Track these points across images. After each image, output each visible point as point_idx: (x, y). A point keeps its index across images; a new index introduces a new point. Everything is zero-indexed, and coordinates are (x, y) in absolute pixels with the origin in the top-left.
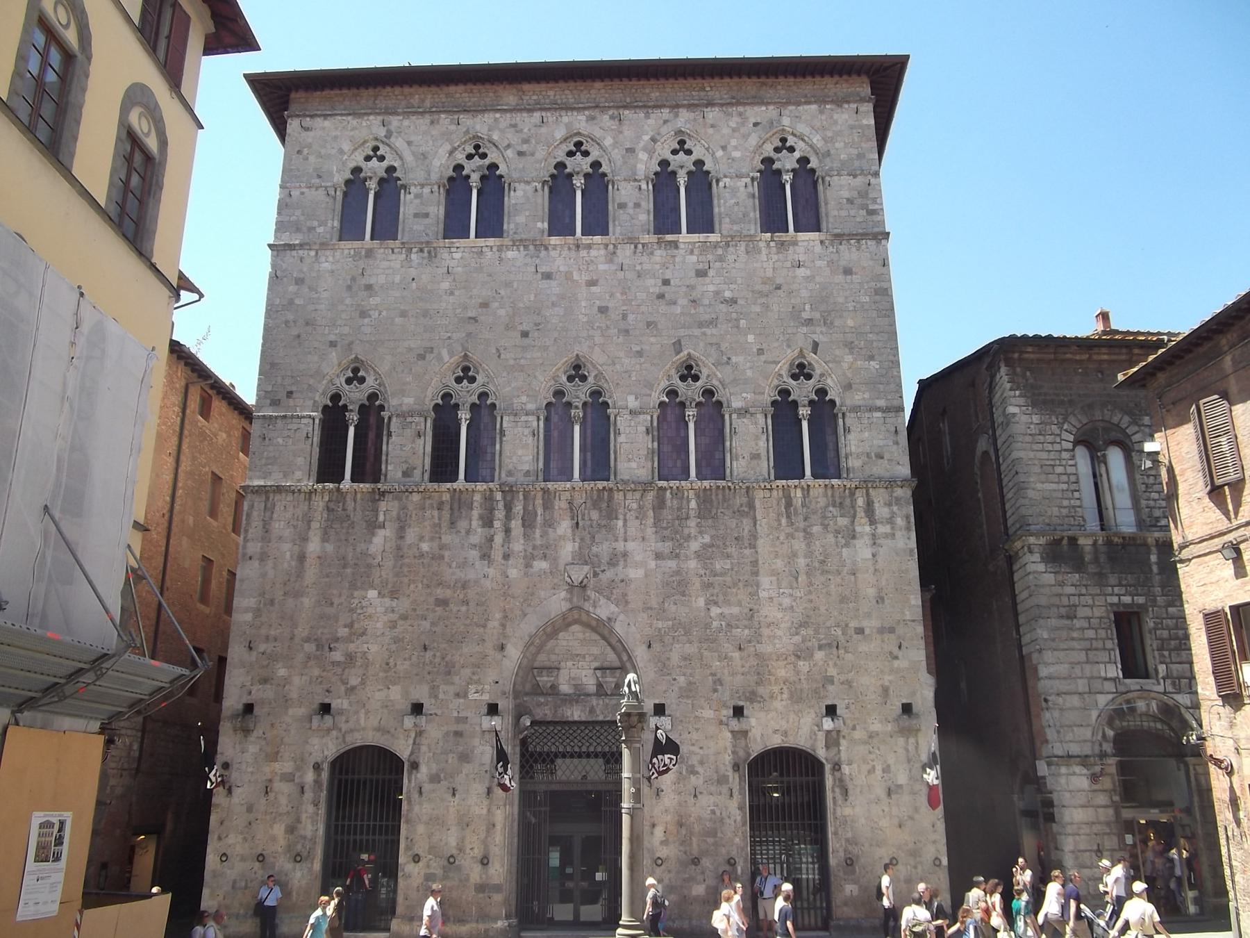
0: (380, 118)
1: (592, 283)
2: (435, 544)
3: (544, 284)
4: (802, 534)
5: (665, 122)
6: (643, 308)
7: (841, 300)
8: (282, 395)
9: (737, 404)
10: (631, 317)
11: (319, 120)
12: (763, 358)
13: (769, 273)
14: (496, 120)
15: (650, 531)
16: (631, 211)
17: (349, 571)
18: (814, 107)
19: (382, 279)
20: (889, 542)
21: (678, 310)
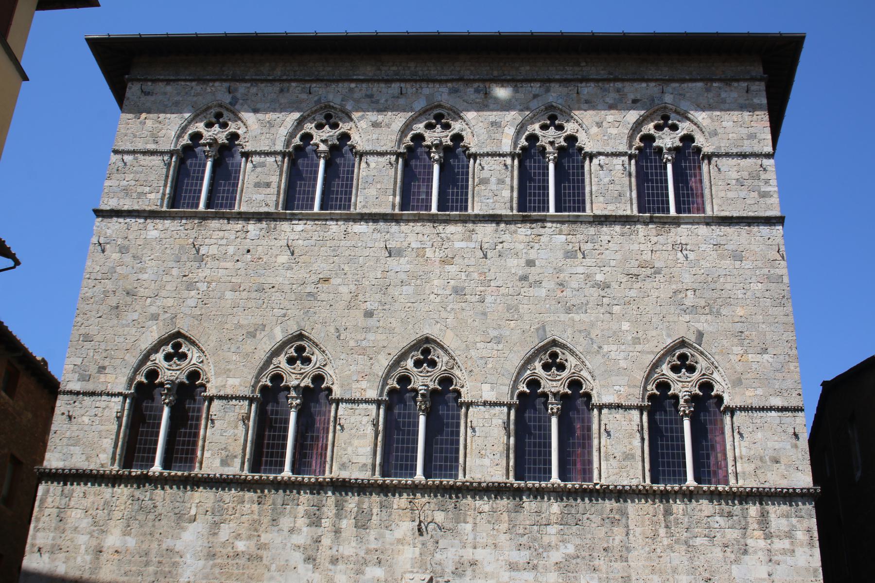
0: (226, 85)
1: (446, 261)
2: (252, 543)
3: (392, 263)
4: (684, 547)
5: (535, 96)
6: (503, 290)
7: (728, 286)
8: (93, 369)
9: (607, 399)
10: (489, 299)
11: (161, 85)
12: (639, 348)
13: (647, 256)
14: (351, 90)
15: (503, 538)
16: (494, 187)
17: (151, 569)
18: (700, 85)
19: (213, 250)
20: (788, 559)
21: (543, 292)
